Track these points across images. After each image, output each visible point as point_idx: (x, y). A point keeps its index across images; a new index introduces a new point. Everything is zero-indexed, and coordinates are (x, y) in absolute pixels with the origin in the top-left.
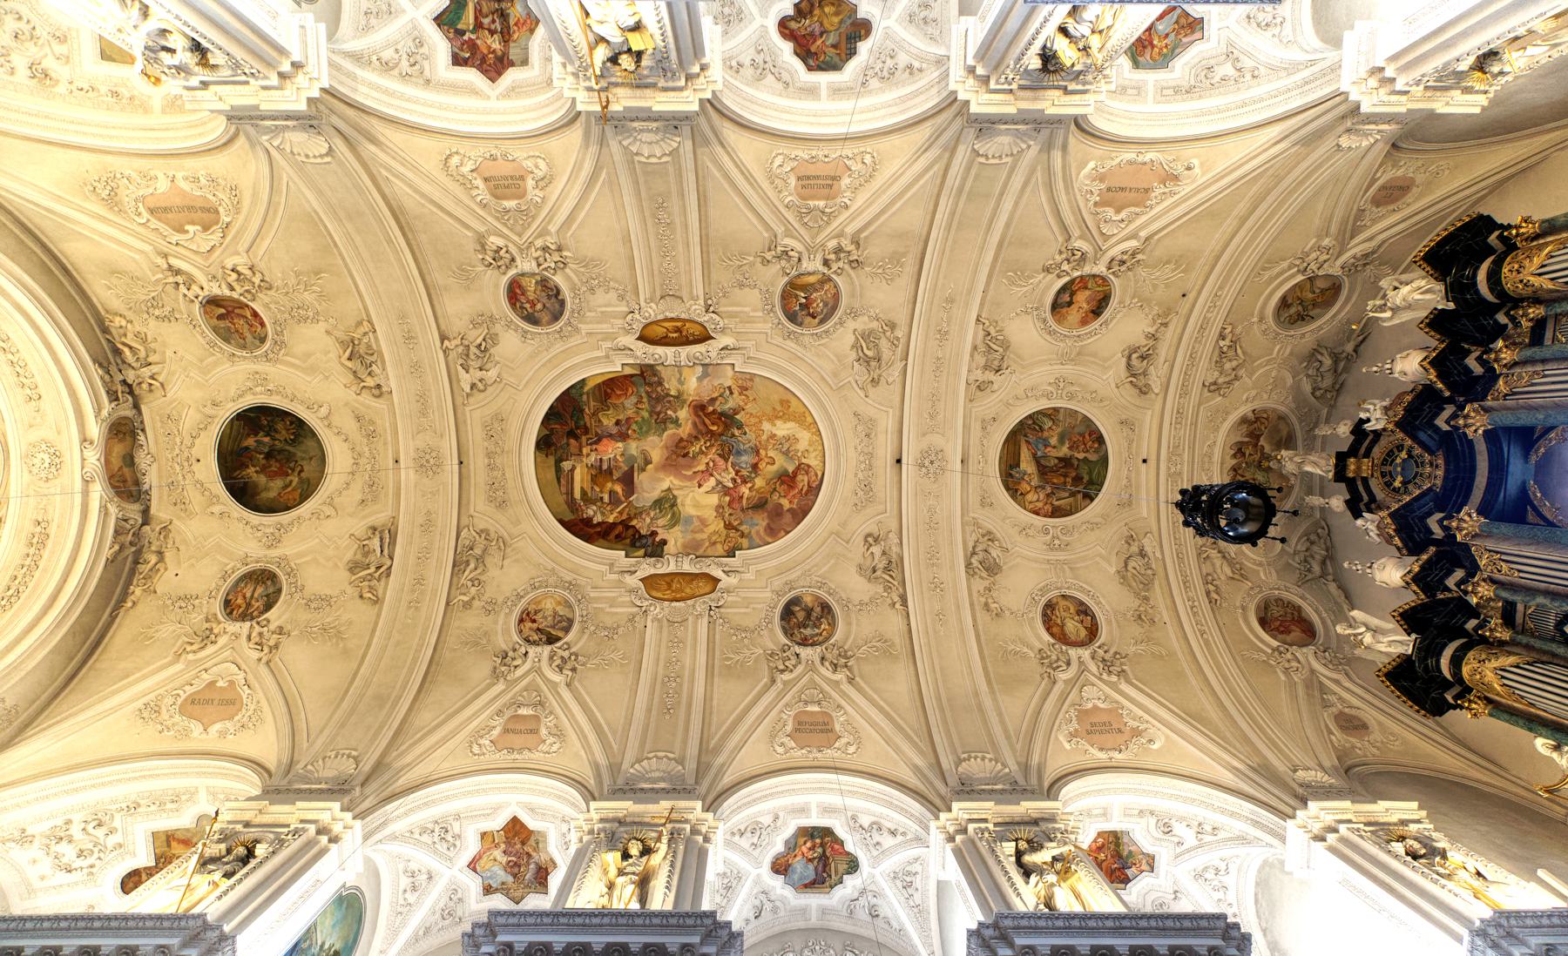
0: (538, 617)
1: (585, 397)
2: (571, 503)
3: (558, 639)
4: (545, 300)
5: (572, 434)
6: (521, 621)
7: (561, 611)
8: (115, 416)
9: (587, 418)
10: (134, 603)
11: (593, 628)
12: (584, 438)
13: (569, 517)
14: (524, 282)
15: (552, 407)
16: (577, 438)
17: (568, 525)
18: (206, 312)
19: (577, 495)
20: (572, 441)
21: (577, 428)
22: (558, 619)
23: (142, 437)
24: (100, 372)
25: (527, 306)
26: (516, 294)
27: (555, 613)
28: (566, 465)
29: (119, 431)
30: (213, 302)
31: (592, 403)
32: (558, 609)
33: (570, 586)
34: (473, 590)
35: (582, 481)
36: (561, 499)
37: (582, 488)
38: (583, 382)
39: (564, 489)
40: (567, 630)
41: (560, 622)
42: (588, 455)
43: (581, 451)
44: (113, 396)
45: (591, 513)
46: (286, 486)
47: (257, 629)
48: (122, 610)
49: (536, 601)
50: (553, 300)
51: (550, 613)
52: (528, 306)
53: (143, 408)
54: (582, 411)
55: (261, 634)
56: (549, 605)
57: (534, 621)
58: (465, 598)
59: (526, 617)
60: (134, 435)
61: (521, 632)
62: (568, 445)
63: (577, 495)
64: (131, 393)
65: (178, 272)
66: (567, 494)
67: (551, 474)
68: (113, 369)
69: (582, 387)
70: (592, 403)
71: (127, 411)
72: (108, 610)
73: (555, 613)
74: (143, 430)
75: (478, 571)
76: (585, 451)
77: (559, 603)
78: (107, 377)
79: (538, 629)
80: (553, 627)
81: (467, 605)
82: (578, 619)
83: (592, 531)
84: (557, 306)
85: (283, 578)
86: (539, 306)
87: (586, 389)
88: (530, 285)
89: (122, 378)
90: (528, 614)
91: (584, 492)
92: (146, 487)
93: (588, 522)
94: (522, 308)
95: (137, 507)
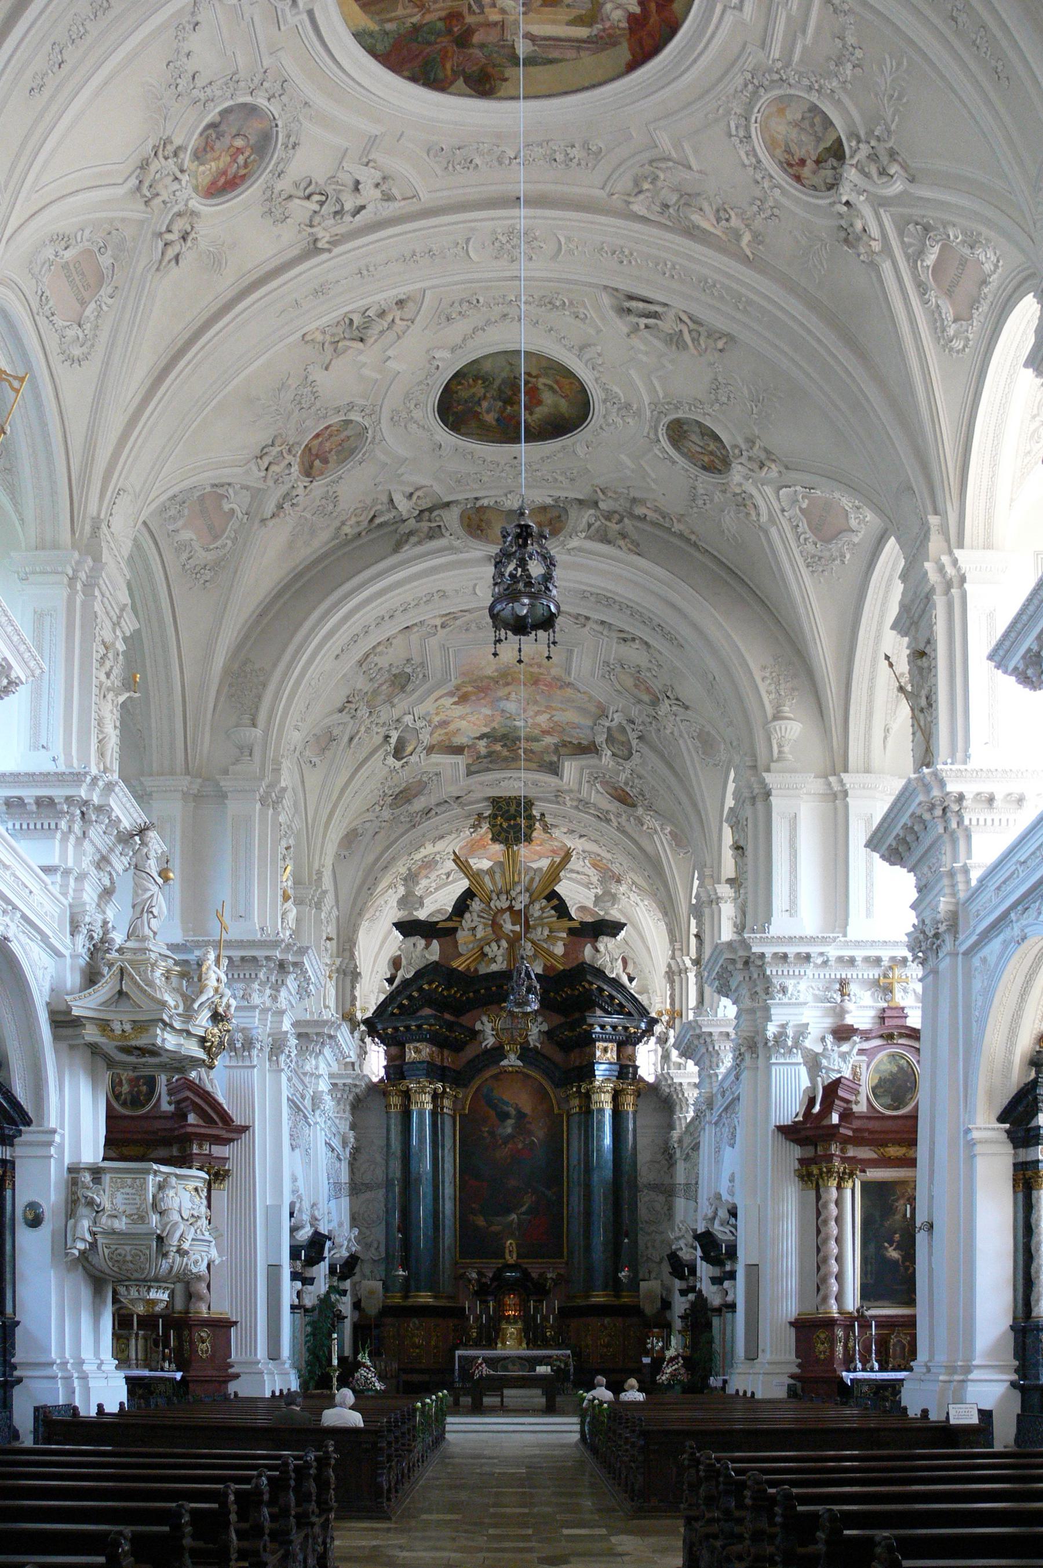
0: (799, 153)
1: (389, 26)
2: (602, 43)
3: (839, 141)
4: (227, 140)
5: (463, 40)
6: (798, 178)
7: (794, 113)
8: (461, 532)
9: (428, 18)
10: (693, 533)
11: (835, 83)
12: (470, 19)
13: (623, 53)
14: (205, 180)
15: (413, 79)
16: (469, 32)
17: (641, 57)
18: (322, 474)
19: (582, 32)
20: (476, 38)
21: (449, 31)
22: (806, 124)
23: (485, 502)
24: (406, 547)
25: (241, 159)
26: (226, 183)
27: (796, 124)
28: (522, 48)
29: (479, 527)
30: (308, 472)
31: (400, 12)
32: (789, 117)
33: (755, 86)
34: (734, 222)
35: (554, 22)
36: (587, 59)
37: (570, 23)
38: (358, 36)
39: (571, 54)
40: (828, 123)
41: (813, 125)
42: (503, 11)
43: (496, 24)
44: (435, 533)
45: (618, 15)
46: (551, 388)
47: (743, 460)
48: (700, 543)
49: (771, 146)
50: (223, 127)
51: (794, 134)
52: (241, 159)
53: (446, 500)
54: (416, 28)
55: (750, 458)
56: (781, 129)
57: (802, 162)
58: (747, 237)
59: (794, 167)
60: (482, 509)
61: (815, 188)
62: (482, 46)
63: (582, 32)
64: (430, 510)
65: (280, 507)
66: (579, 49)
67: (539, 72)
68: (404, 529)
69: (371, 35)
70: (400, 12)
71: (451, 518)
72: (697, 554)
73: (796, 124)
74: (477, 499)
75: (706, 206)
76: (494, 17)
77: (781, 111)
78: (414, 539)
79: (818, 162)
80: (819, 140)
81: (757, 238)
82: (814, 98)
83: (654, 19)
84: (232, 117)
85: (680, 415)
86: (239, 143)
87: (373, 26)
88: (208, 170)
89: (412, 521)
90: (790, 165)
91: (579, 21)
92: (549, 501)
93: (636, 22)
94: (246, 165)
95: (573, 513)
